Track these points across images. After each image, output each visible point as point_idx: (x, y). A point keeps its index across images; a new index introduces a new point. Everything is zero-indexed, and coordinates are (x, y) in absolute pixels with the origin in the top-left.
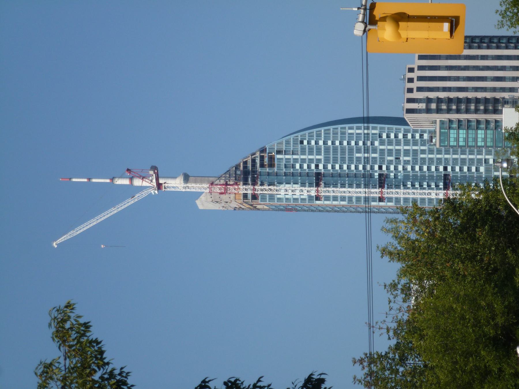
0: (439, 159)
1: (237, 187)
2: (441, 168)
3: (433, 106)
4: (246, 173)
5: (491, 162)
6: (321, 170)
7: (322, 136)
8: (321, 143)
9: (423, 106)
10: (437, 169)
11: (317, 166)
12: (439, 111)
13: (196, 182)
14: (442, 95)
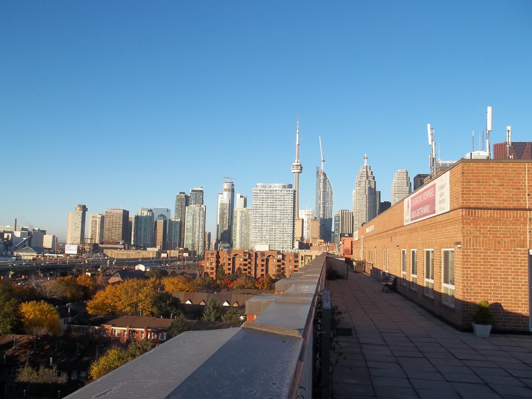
3: (342, 214)
9: (342, 213)
12: (342, 215)
13: (298, 147)
14: (344, 216)
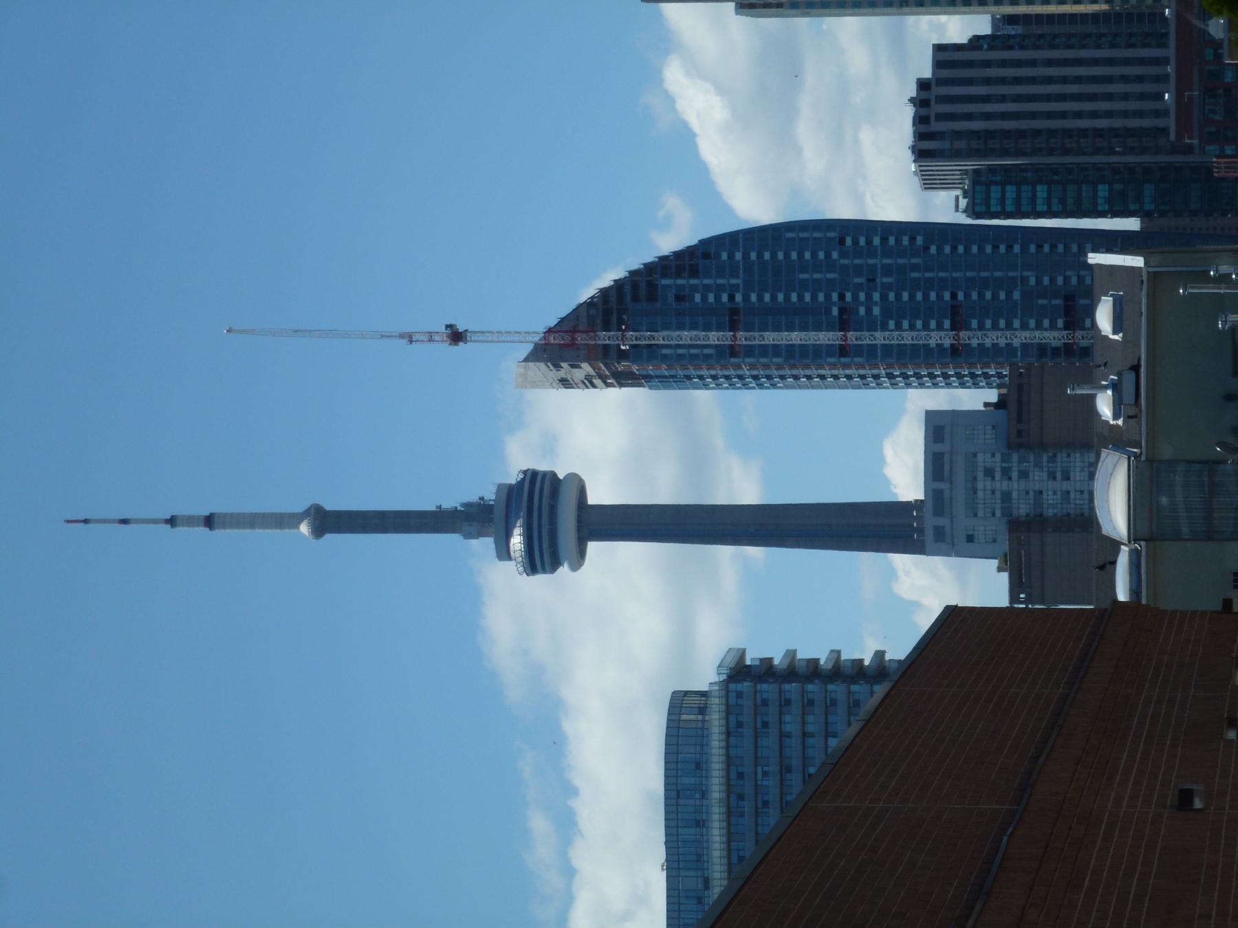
0: (944, 280)
1: (592, 334)
2: (947, 296)
4: (607, 313)
5: (1032, 281)
6: (738, 303)
7: (741, 245)
8: (738, 256)
10: (940, 297)
11: (732, 298)
